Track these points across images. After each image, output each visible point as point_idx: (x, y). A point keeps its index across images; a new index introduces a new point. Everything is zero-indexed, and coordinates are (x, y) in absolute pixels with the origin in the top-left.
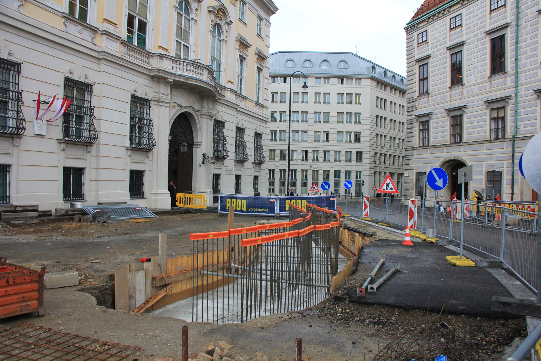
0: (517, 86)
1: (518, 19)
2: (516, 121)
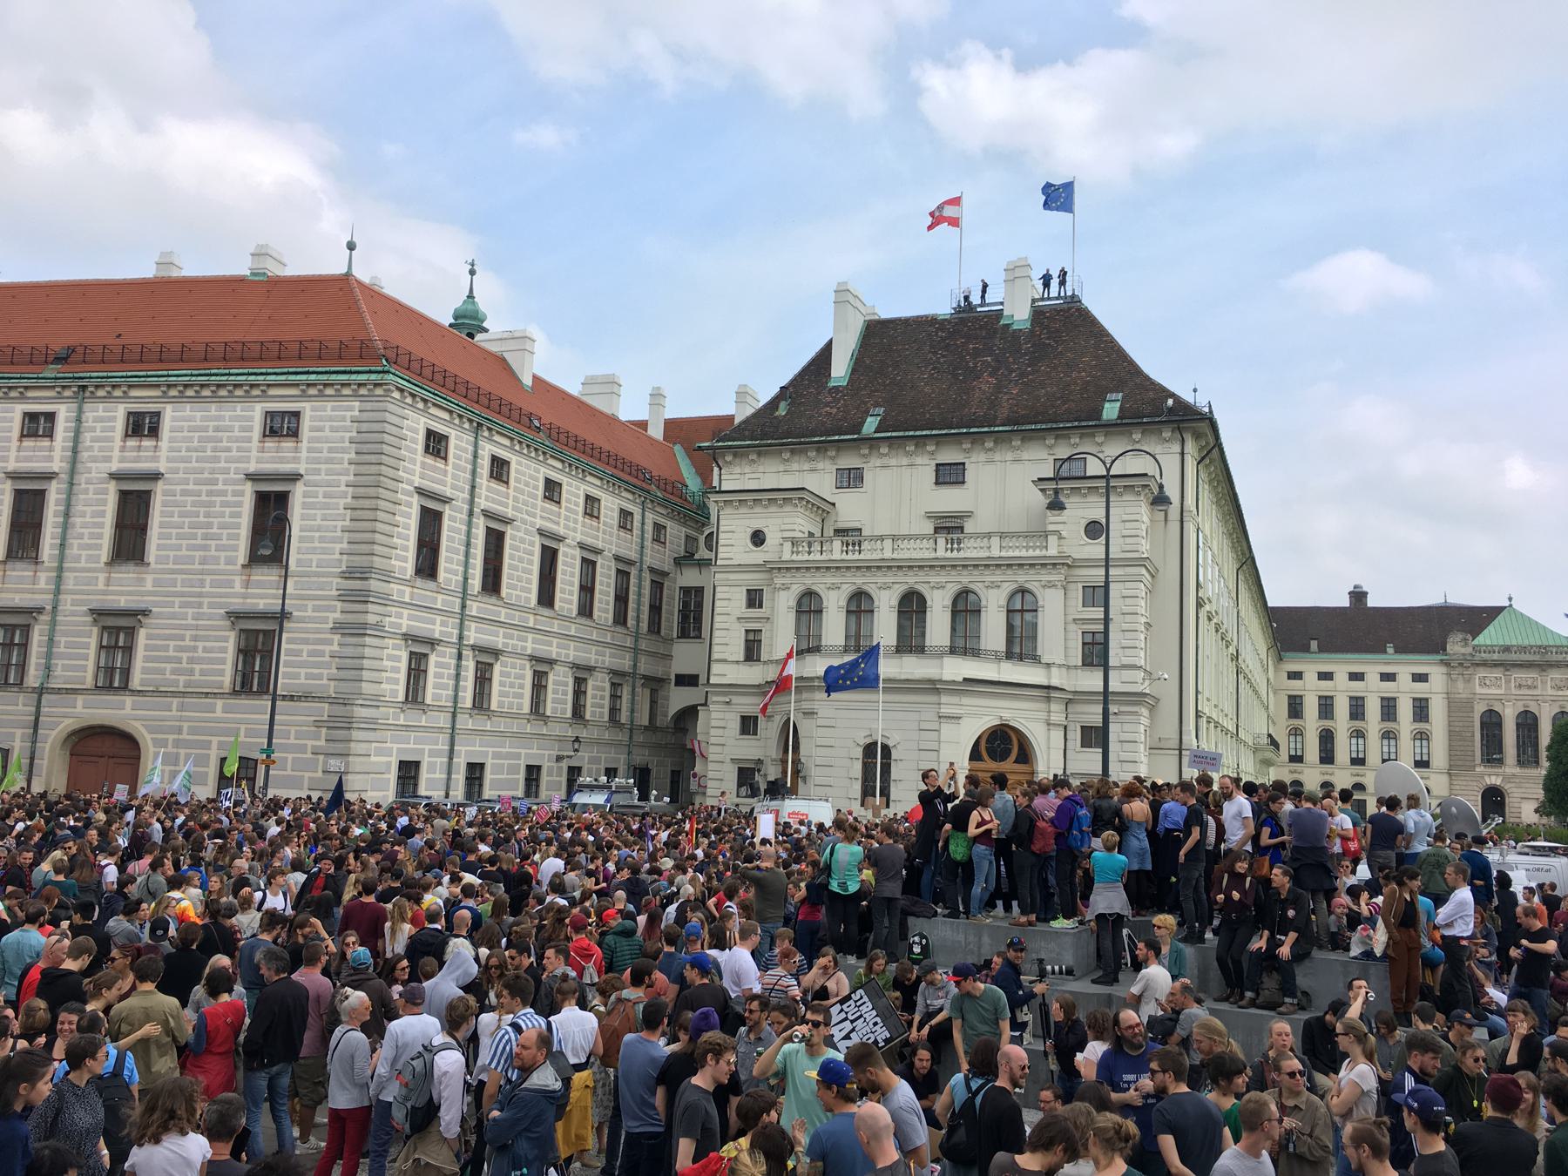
0: (57, 592)
1: (73, 472)
2: (49, 656)
